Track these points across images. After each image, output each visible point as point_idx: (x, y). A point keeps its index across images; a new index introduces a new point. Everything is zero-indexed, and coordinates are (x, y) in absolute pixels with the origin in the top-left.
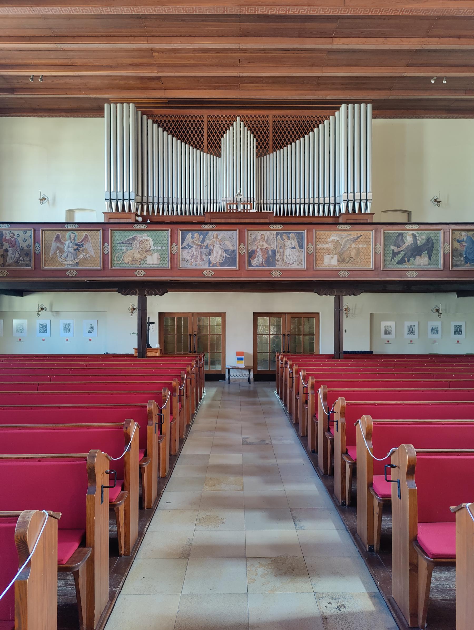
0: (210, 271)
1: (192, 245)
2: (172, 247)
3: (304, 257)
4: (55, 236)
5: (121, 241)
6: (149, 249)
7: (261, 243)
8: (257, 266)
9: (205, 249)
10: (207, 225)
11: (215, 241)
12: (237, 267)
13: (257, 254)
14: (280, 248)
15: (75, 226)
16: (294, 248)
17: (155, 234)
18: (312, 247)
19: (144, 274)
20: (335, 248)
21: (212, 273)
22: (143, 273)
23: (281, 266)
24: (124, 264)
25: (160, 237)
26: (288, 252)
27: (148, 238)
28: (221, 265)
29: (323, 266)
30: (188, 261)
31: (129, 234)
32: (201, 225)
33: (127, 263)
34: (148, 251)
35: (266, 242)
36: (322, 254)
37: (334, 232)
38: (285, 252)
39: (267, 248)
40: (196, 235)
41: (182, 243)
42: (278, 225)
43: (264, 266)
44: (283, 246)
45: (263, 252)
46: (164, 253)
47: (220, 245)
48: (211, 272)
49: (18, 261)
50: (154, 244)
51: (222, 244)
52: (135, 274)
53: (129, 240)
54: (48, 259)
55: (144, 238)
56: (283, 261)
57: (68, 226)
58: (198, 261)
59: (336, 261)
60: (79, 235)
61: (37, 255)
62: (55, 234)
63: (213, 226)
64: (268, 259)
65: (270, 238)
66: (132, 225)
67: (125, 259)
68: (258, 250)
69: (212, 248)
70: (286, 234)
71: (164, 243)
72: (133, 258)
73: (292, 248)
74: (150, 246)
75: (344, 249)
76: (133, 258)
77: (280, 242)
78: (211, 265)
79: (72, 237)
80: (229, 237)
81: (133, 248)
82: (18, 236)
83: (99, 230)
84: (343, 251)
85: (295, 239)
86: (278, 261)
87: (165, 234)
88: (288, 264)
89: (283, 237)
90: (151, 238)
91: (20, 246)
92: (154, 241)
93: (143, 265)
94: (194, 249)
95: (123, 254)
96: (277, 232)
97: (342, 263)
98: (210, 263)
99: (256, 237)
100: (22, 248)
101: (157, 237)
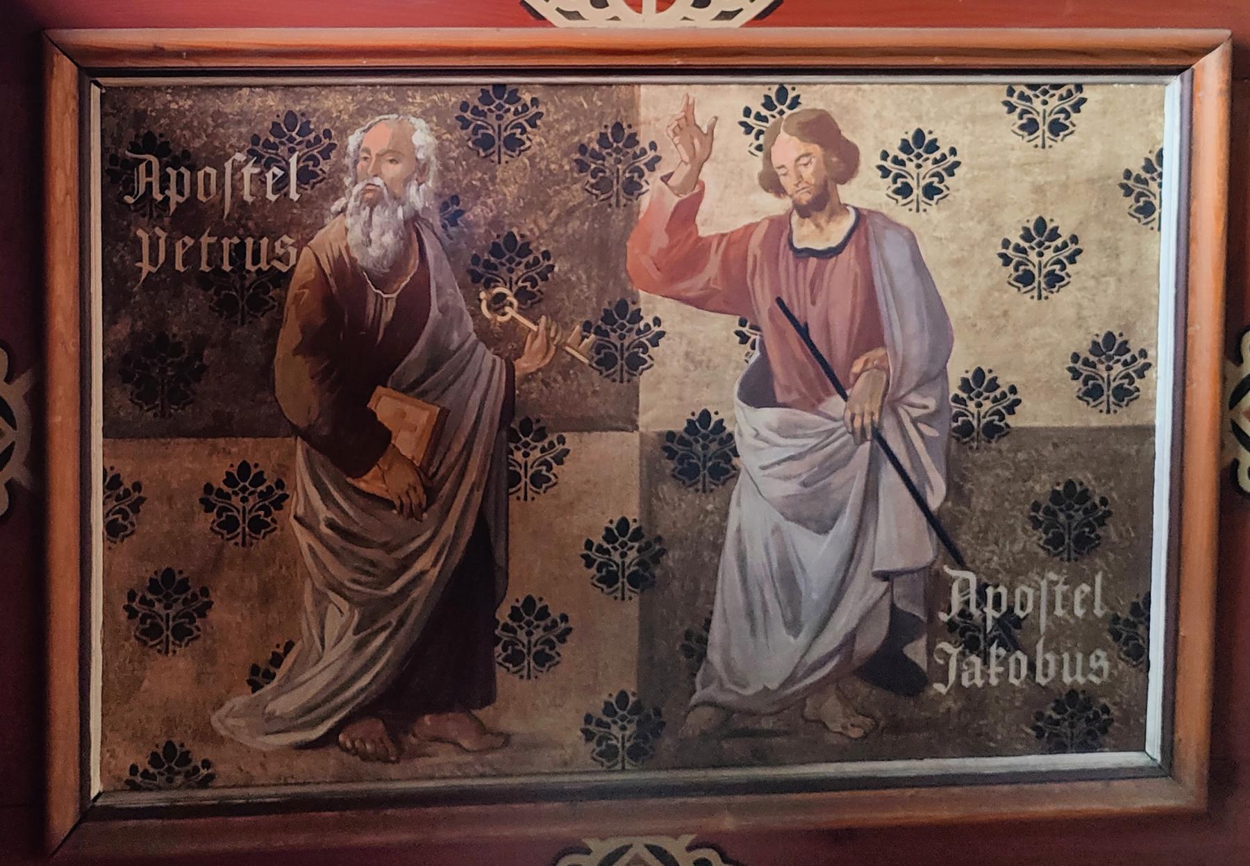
49: (916, 652)
82: (919, 172)
91: (958, 369)
100: (980, 410)
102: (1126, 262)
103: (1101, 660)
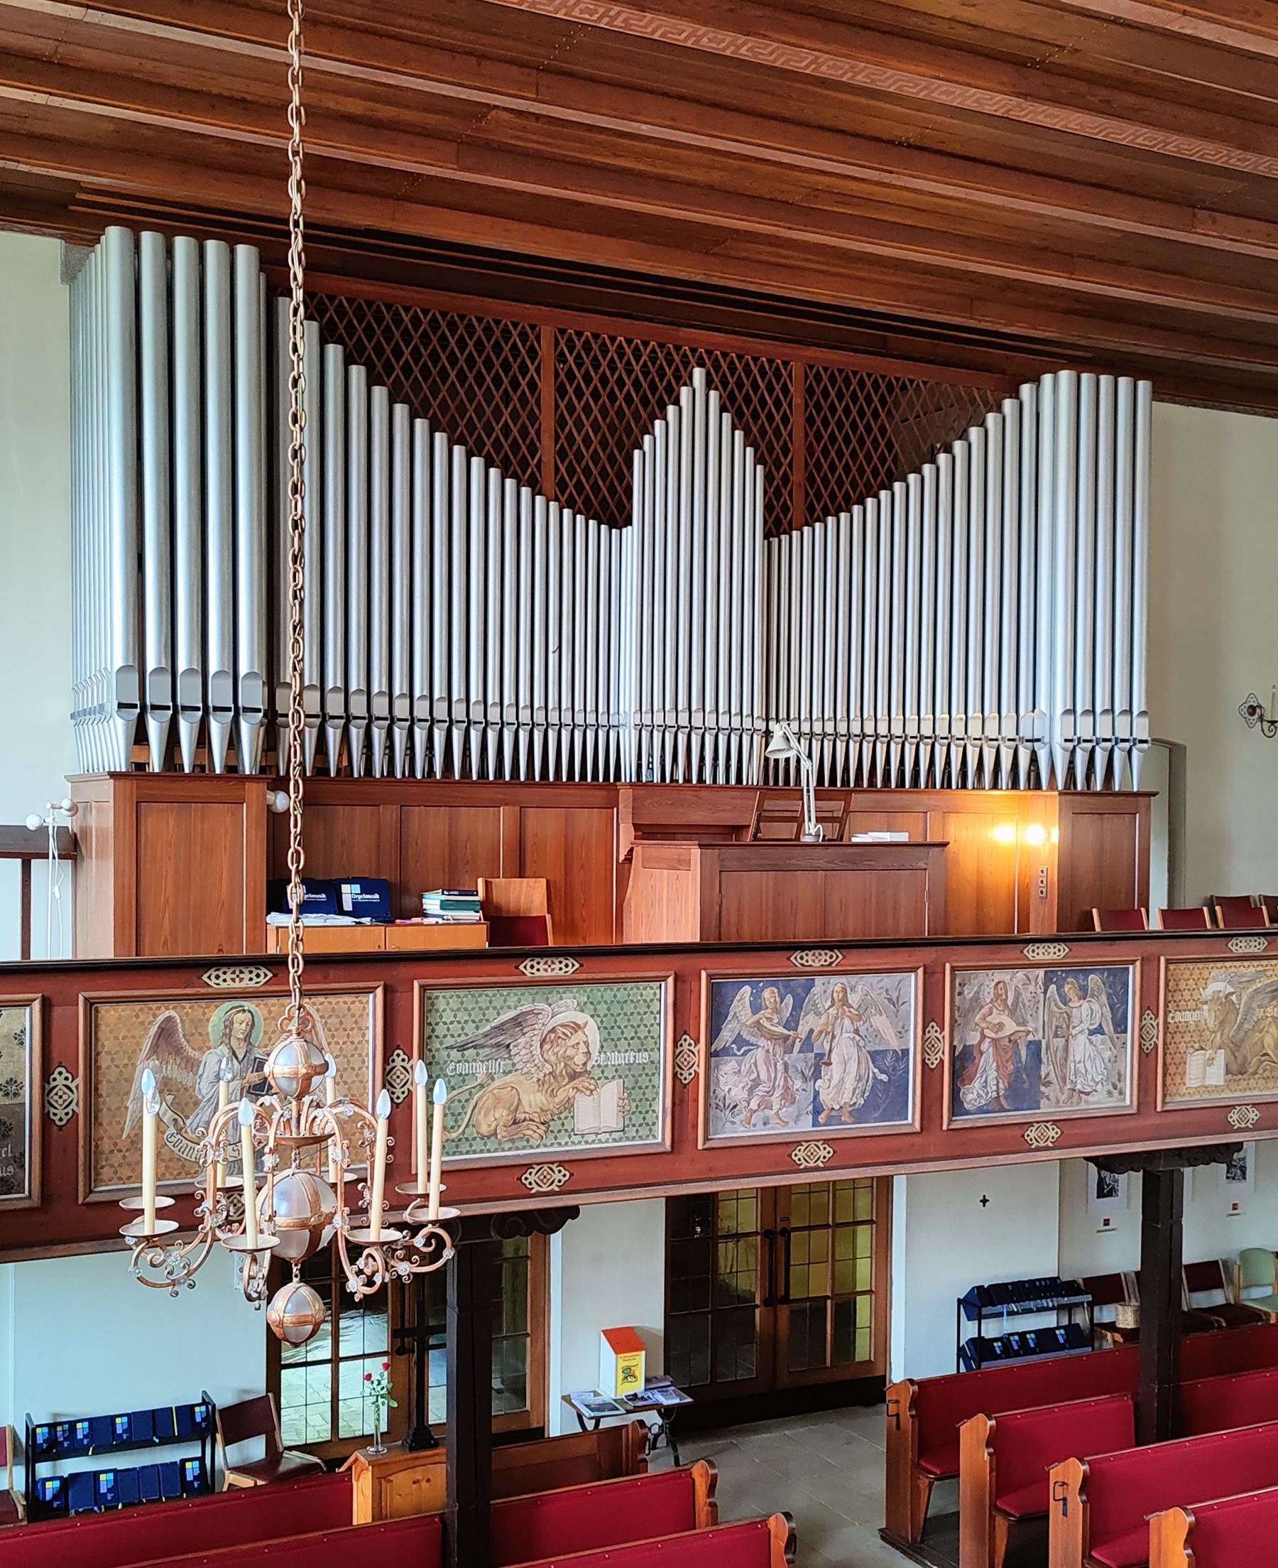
0: (819, 1144)
1: (753, 1040)
2: (678, 1051)
3: (1129, 1065)
4: (154, 1030)
5: (463, 1038)
6: (585, 1064)
7: (994, 1019)
8: (981, 1110)
9: (799, 1052)
10: (810, 953)
11: (836, 1018)
12: (913, 1119)
13: (981, 1064)
14: (1056, 1036)
15: (253, 975)
16: (1099, 1030)
17: (608, 995)
18: (1155, 1024)
19: (563, 1180)
20: (1222, 1023)
21: (825, 1152)
22: (560, 1176)
23: (1058, 1101)
24: (474, 1139)
25: (629, 1008)
26: (1080, 1046)
27: (581, 1018)
28: (859, 1114)
29: (1184, 1094)
30: (735, 1107)
31: (498, 1002)
32: (788, 954)
33: (489, 1137)
34: (580, 1074)
35: (1012, 1013)
36: (1182, 1047)
37: (1219, 965)
38: (1071, 1050)
39: (1012, 1038)
40: (769, 994)
41: (713, 1033)
42: (1052, 945)
43: (1003, 1110)
44: (1064, 1026)
45: (1001, 1050)
46: (643, 1081)
47: (857, 1031)
48: (822, 1147)
50: (606, 1040)
51: (862, 1031)
52: (527, 1183)
53: (500, 1028)
54: (115, 1144)
55: (561, 1019)
56: (1065, 1083)
57: (217, 977)
58: (776, 1107)
59: (1223, 1071)
60: (270, 1018)
61: (60, 1128)
62: (155, 1016)
63: (831, 957)
64: (1016, 1080)
65: (1026, 996)
66: (514, 962)
67: (481, 1117)
68: (984, 1046)
69: (827, 1047)
70: (1076, 978)
71: (646, 1038)
72: (517, 1109)
73: (1092, 1033)
74: (588, 1053)
75: (1246, 1026)
76: (517, 1109)
77: (1056, 1009)
78: (822, 1118)
79: (240, 1028)
80: (889, 999)
81: (514, 1065)
83: (372, 990)
84: (1241, 1034)
85: (1104, 998)
86: (1048, 1084)
87: (649, 991)
88: (1080, 1092)
89: (1066, 988)
90: (592, 1016)
92: (605, 1028)
93: (556, 1138)
94: (760, 1054)
95: (470, 1093)
96: (1046, 972)
97: (1240, 1076)
98: (817, 1111)
99: (977, 992)
101: (616, 1009)
102: (16, 1057)
103: (11, 1169)
